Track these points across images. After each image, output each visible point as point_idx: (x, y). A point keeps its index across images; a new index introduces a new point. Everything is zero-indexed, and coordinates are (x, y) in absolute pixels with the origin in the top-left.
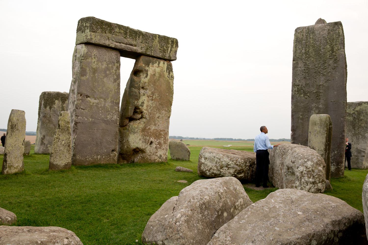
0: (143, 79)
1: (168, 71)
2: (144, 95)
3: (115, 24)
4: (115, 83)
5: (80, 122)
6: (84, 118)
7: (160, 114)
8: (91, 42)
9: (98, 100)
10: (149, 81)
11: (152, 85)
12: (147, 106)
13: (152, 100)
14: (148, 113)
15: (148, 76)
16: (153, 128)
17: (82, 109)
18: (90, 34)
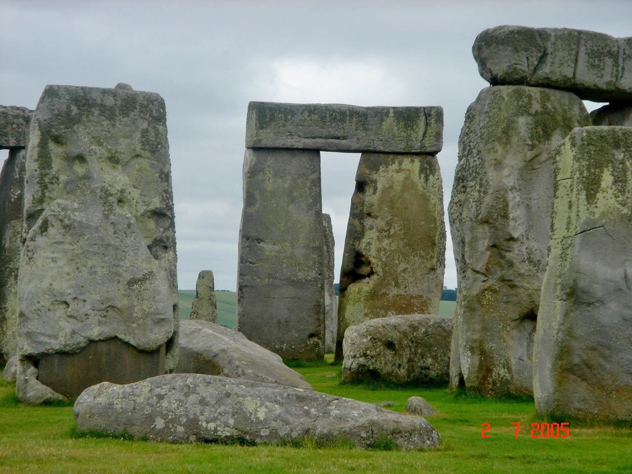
0: (371, 198)
1: (423, 176)
2: (371, 228)
3: (300, 106)
4: (310, 212)
5: (247, 286)
6: (255, 278)
7: (407, 263)
8: (258, 146)
9: (280, 245)
10: (381, 202)
11: (386, 209)
12: (379, 250)
13: (389, 237)
14: (380, 264)
15: (378, 191)
16: (393, 292)
17: (250, 263)
18: (257, 133)
